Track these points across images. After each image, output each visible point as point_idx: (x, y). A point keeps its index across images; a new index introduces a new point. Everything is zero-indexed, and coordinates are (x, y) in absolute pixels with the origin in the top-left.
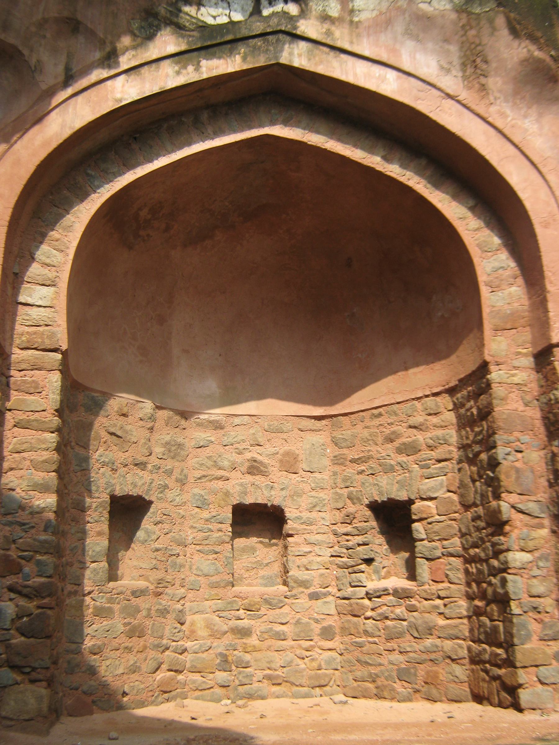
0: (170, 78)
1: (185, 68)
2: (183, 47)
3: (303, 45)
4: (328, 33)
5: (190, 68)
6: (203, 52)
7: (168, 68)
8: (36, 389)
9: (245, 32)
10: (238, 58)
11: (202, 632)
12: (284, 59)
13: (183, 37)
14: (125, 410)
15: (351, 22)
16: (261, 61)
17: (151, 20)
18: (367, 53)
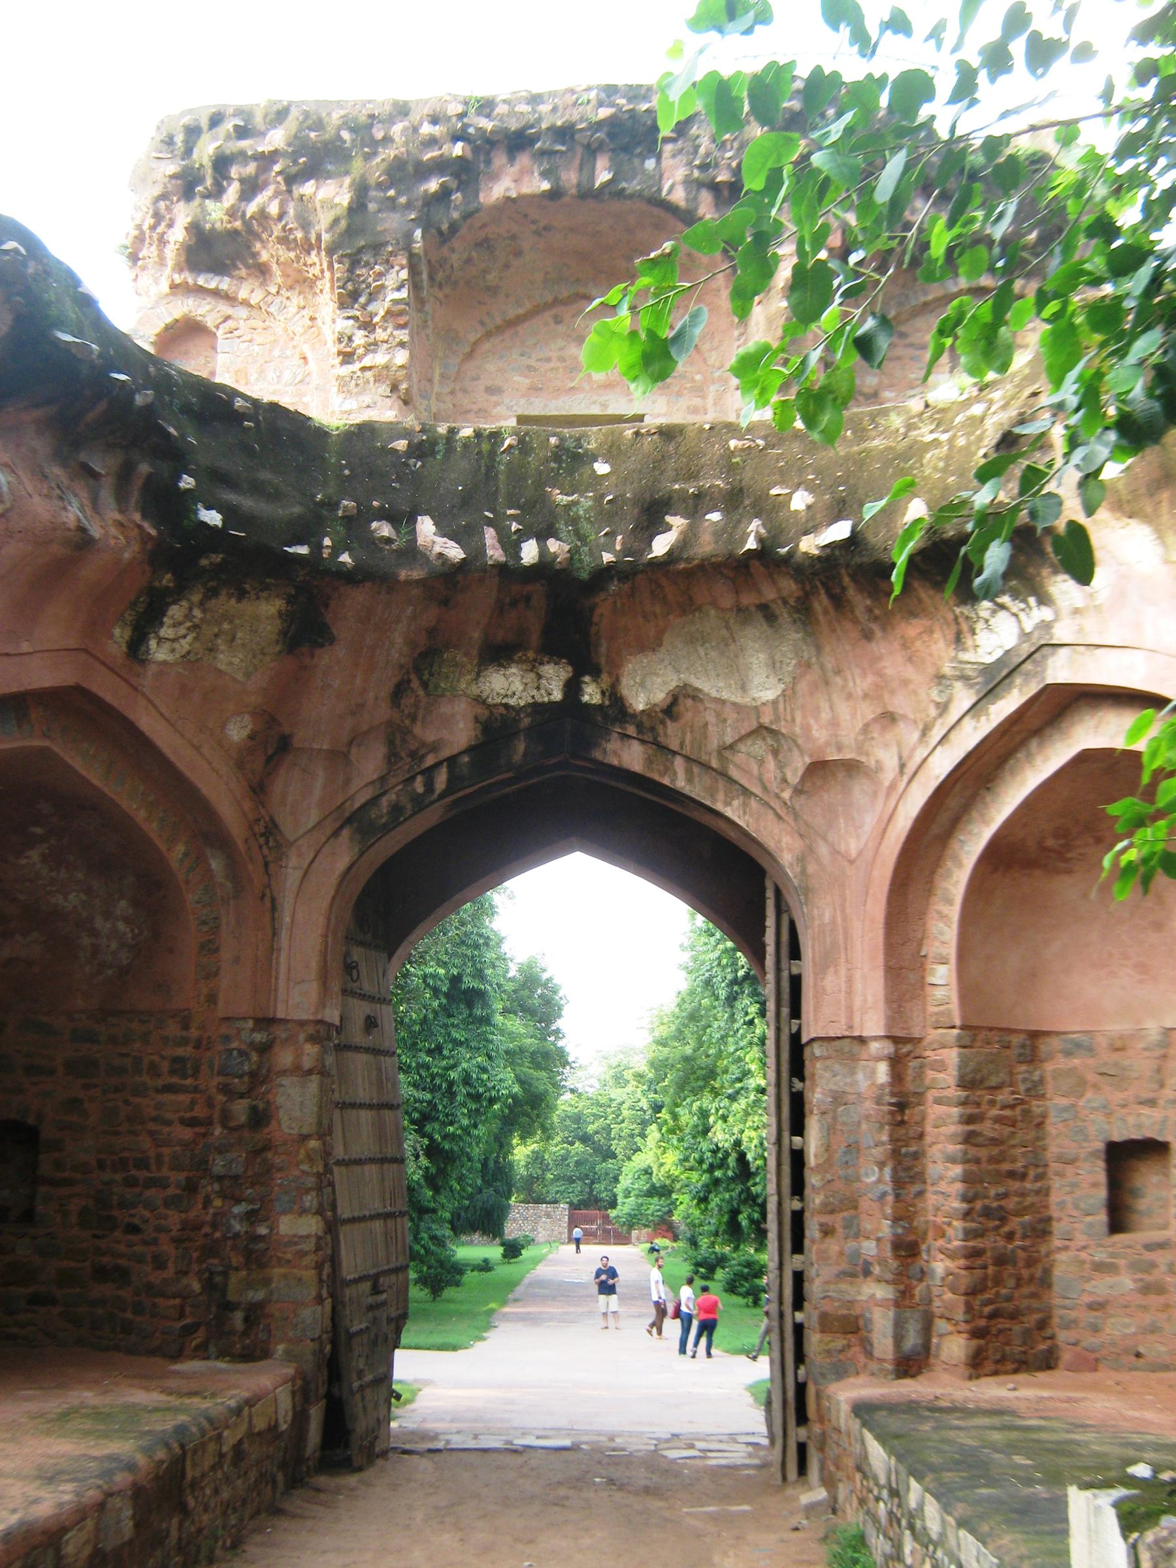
0: (971, 735)
2: (974, 699)
3: (1063, 651)
4: (1081, 630)
5: (983, 718)
6: (990, 696)
7: (968, 723)
8: (941, 1066)
10: (1015, 692)
12: (1049, 681)
14: (1119, 1044)
16: (1033, 689)
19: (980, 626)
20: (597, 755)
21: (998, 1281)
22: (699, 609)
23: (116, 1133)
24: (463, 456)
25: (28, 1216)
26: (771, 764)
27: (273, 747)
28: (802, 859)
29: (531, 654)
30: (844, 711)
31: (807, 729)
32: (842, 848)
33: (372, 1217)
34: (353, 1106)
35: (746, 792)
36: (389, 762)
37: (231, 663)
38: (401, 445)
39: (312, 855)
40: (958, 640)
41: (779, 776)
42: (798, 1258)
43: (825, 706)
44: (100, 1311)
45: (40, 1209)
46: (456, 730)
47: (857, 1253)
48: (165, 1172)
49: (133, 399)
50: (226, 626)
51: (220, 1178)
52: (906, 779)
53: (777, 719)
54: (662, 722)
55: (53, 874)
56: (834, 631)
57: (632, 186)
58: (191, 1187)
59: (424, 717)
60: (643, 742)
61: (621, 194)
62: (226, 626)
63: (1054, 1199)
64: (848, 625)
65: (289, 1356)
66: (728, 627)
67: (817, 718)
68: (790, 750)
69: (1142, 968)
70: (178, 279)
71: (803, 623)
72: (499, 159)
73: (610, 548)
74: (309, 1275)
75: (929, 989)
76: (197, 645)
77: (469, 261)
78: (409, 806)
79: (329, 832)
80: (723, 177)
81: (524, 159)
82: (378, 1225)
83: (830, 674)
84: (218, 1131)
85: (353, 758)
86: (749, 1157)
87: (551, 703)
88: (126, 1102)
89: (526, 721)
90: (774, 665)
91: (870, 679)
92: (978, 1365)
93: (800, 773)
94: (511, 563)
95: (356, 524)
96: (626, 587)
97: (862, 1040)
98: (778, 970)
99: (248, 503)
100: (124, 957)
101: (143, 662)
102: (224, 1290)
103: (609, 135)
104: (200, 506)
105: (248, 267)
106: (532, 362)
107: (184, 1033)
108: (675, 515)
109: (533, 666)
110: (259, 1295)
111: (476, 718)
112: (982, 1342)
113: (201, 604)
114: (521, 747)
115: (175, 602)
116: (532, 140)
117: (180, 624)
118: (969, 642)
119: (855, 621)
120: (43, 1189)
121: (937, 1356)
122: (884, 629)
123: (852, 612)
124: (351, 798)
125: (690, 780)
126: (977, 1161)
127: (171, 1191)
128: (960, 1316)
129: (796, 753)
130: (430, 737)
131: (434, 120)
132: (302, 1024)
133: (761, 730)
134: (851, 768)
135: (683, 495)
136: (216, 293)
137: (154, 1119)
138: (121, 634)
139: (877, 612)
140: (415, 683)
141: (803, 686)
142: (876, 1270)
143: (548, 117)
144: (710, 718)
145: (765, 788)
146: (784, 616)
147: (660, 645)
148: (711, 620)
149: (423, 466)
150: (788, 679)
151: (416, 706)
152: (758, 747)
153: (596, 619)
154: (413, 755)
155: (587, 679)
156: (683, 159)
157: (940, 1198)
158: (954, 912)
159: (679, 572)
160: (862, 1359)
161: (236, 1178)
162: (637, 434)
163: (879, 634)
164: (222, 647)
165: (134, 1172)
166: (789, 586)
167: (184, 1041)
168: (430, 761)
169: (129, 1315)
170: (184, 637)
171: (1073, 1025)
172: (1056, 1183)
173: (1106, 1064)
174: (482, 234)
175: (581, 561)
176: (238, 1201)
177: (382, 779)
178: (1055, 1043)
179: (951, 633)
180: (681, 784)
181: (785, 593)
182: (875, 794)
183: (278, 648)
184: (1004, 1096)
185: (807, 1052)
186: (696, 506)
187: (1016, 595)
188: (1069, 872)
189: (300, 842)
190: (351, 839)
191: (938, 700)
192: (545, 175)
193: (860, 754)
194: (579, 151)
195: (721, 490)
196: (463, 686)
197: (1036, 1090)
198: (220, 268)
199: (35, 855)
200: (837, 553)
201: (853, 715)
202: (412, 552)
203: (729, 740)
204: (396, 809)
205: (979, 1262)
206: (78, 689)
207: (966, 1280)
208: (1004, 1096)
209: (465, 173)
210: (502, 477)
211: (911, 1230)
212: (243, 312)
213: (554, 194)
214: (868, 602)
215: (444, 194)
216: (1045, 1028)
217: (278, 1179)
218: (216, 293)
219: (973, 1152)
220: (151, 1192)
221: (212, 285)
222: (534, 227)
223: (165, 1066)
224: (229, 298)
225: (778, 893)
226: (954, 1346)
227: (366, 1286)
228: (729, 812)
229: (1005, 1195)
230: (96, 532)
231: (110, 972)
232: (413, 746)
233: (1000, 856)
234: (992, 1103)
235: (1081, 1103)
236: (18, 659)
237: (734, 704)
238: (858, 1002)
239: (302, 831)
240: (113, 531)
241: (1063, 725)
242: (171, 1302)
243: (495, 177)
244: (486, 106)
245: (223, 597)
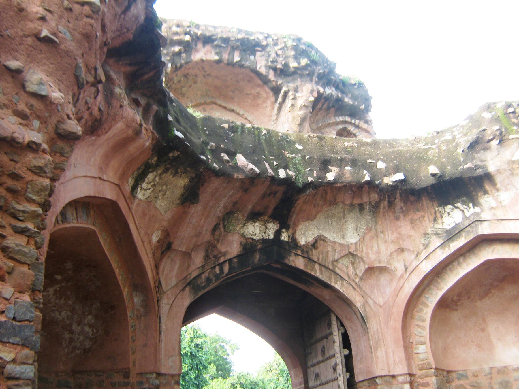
0: (441, 255)
1: (445, 249)
2: (442, 242)
3: (485, 223)
4: (494, 215)
5: (447, 249)
6: (450, 241)
9: (463, 227)
10: (463, 238)
12: (480, 233)
13: (440, 237)
14: (476, 374)
15: (502, 206)
16: (472, 236)
17: (427, 236)
19: (446, 214)
20: (286, 261)
22: (336, 204)
24: (248, 135)
26: (351, 268)
27: (166, 247)
28: (363, 306)
29: (266, 218)
30: (383, 247)
31: (367, 254)
32: (377, 301)
36: (205, 259)
37: (161, 205)
38: (226, 126)
39: (173, 299)
40: (435, 220)
41: (354, 273)
43: (375, 245)
46: (232, 248)
50: (164, 188)
52: (408, 273)
53: (356, 250)
54: (311, 250)
55: (57, 301)
56: (384, 216)
57: (247, 64)
59: (222, 241)
60: (303, 257)
61: (242, 66)
64: (391, 214)
66: (344, 213)
67: (372, 250)
68: (359, 262)
69: (479, 346)
71: (374, 212)
72: (200, 45)
73: (311, 175)
75: (415, 356)
76: (152, 194)
77: (179, 81)
78: (214, 279)
79: (181, 288)
80: (279, 66)
81: (208, 47)
83: (379, 233)
85: (192, 256)
87: (269, 239)
89: (260, 246)
91: (395, 235)
93: (363, 272)
94: (276, 176)
95: (216, 153)
96: (314, 192)
97: (393, 376)
100: (87, 344)
103: (241, 44)
104: (175, 129)
107: (126, 380)
108: (332, 166)
111: (241, 243)
114: (257, 256)
115: (152, 172)
117: (150, 183)
118: (440, 221)
119: (394, 212)
122: (404, 216)
123: (394, 208)
124: (190, 274)
129: (362, 263)
130: (223, 250)
131: (178, 26)
134: (383, 270)
135: (336, 160)
138: (131, 181)
139: (404, 209)
141: (367, 238)
143: (220, 33)
144: (330, 249)
145: (349, 277)
146: (367, 208)
147: (315, 218)
148: (337, 210)
149: (234, 136)
150: (362, 235)
151: (220, 235)
152: (346, 261)
153: (296, 205)
154: (215, 257)
155: (284, 230)
156: (264, 58)
158: (427, 324)
159: (336, 187)
162: (309, 136)
163: (402, 218)
164: (160, 197)
166: (375, 196)
168: (222, 260)
170: (149, 189)
171: (460, 368)
173: (473, 382)
174: (186, 72)
175: (299, 180)
177: (203, 266)
178: (454, 375)
179: (432, 218)
180: (318, 275)
181: (372, 199)
182: (391, 280)
183: (178, 202)
186: (341, 164)
187: (463, 203)
188: (456, 310)
189: (168, 292)
190: (190, 292)
191: (424, 243)
192: (217, 54)
193: (388, 264)
194: (229, 48)
195: (349, 159)
196: (238, 229)
200: (399, 184)
201: (387, 250)
202: (237, 168)
203: (336, 258)
204: (208, 280)
209: (188, 47)
210: (264, 145)
213: (219, 62)
214: (402, 205)
215: (179, 53)
216: (451, 369)
222: (204, 74)
231: (78, 352)
232: (216, 253)
236: (102, 181)
237: (340, 244)
238: (391, 361)
239: (169, 288)
241: (475, 252)
243: (197, 51)
244: (197, 26)
245: (169, 174)
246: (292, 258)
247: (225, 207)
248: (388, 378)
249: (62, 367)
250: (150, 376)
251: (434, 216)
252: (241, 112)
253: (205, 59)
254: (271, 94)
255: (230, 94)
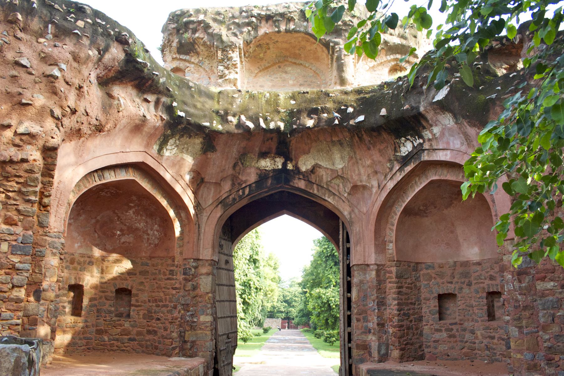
7: (398, 174)
11: (480, 337)
12: (422, 160)
14: (441, 266)
16: (417, 162)
18: (441, 148)
19: (402, 145)
20: (292, 184)
21: (408, 334)
23: (154, 292)
25: (128, 316)
28: (350, 213)
29: (273, 155)
31: (352, 176)
33: (227, 317)
34: (222, 285)
35: (334, 194)
42: (349, 328)
43: (356, 169)
44: (148, 343)
45: (132, 313)
46: (252, 178)
47: (367, 326)
48: (167, 303)
49: (159, 80)
50: (186, 146)
51: (183, 305)
56: (359, 148)
58: (175, 307)
60: (305, 180)
62: (186, 146)
63: (423, 311)
65: (203, 356)
66: (329, 147)
70: (174, 56)
72: (264, 22)
74: (209, 333)
75: (387, 250)
77: (255, 50)
79: (215, 206)
81: (270, 22)
82: (229, 319)
84: (182, 291)
86: (331, 305)
87: (278, 169)
88: (156, 283)
89: (271, 174)
90: (342, 158)
92: (402, 359)
97: (368, 265)
98: (343, 246)
99: (192, 110)
100: (157, 242)
101: (162, 156)
102: (184, 338)
105: (194, 53)
106: (272, 79)
109: (273, 159)
110: (194, 339)
112: (403, 352)
113: (179, 139)
114: (270, 181)
115: (171, 139)
116: (272, 17)
119: (365, 144)
120: (133, 308)
121: (390, 356)
122: (374, 147)
124: (221, 196)
125: (318, 191)
126: (402, 300)
127: (168, 309)
128: (397, 344)
129: (348, 183)
130: (244, 179)
132: (207, 260)
133: (338, 177)
134: (364, 187)
136: (185, 60)
137: (164, 288)
138: (156, 147)
140: (240, 163)
142: (372, 331)
145: (340, 193)
151: (240, 170)
152: (337, 181)
154: (239, 184)
157: (391, 311)
160: (369, 357)
161: (188, 304)
163: (372, 148)
165: (159, 303)
167: (173, 265)
168: (244, 186)
169: (157, 344)
172: (424, 306)
176: (188, 311)
177: (230, 191)
180: (315, 192)
184: (409, 281)
185: (352, 269)
188: (427, 217)
194: (285, 20)
197: (418, 279)
198: (187, 53)
199: (131, 212)
203: (329, 179)
204: (234, 199)
205: (402, 329)
206: (143, 163)
207: (399, 334)
208: (409, 281)
211: (382, 319)
212: (193, 66)
217: (200, 305)
218: (185, 60)
219: (400, 296)
220: (164, 309)
221: (184, 58)
223: (168, 273)
224: (189, 62)
225: (343, 223)
226: (396, 353)
227: (225, 337)
228: (329, 200)
229: (410, 309)
230: (148, 117)
233: (407, 212)
234: (405, 283)
235: (431, 283)
240: (154, 117)
242: (169, 340)
245: (185, 137)
246: (296, 181)
247: (239, 152)
248: (363, 267)
249: (144, 254)
250: (189, 260)
251: (394, 146)
252: (307, 65)
253: (267, 32)
254: (324, 49)
255: (297, 52)
